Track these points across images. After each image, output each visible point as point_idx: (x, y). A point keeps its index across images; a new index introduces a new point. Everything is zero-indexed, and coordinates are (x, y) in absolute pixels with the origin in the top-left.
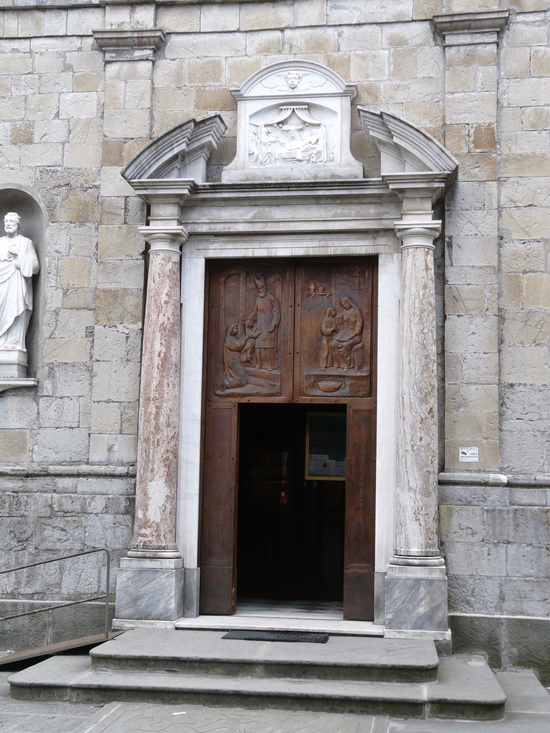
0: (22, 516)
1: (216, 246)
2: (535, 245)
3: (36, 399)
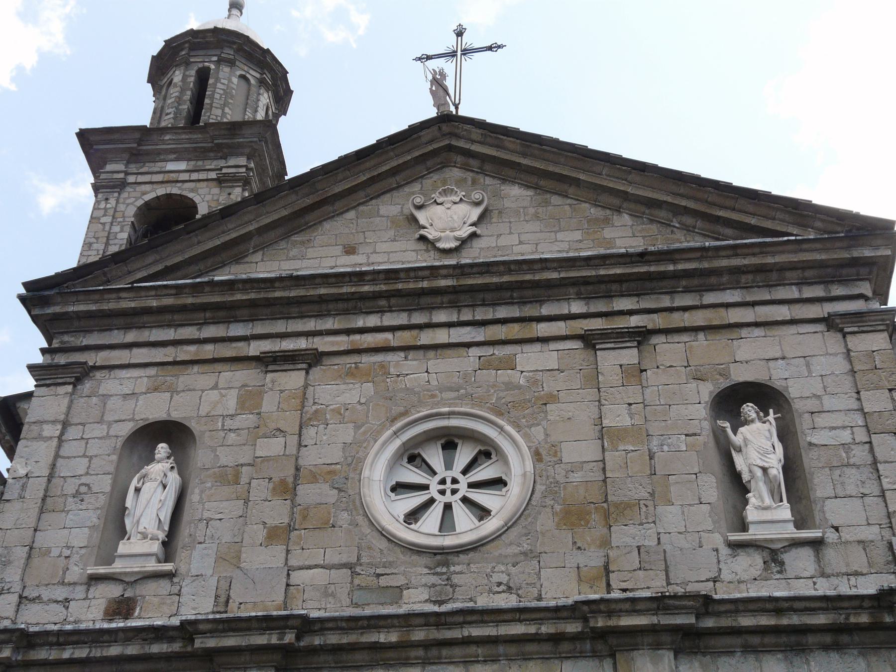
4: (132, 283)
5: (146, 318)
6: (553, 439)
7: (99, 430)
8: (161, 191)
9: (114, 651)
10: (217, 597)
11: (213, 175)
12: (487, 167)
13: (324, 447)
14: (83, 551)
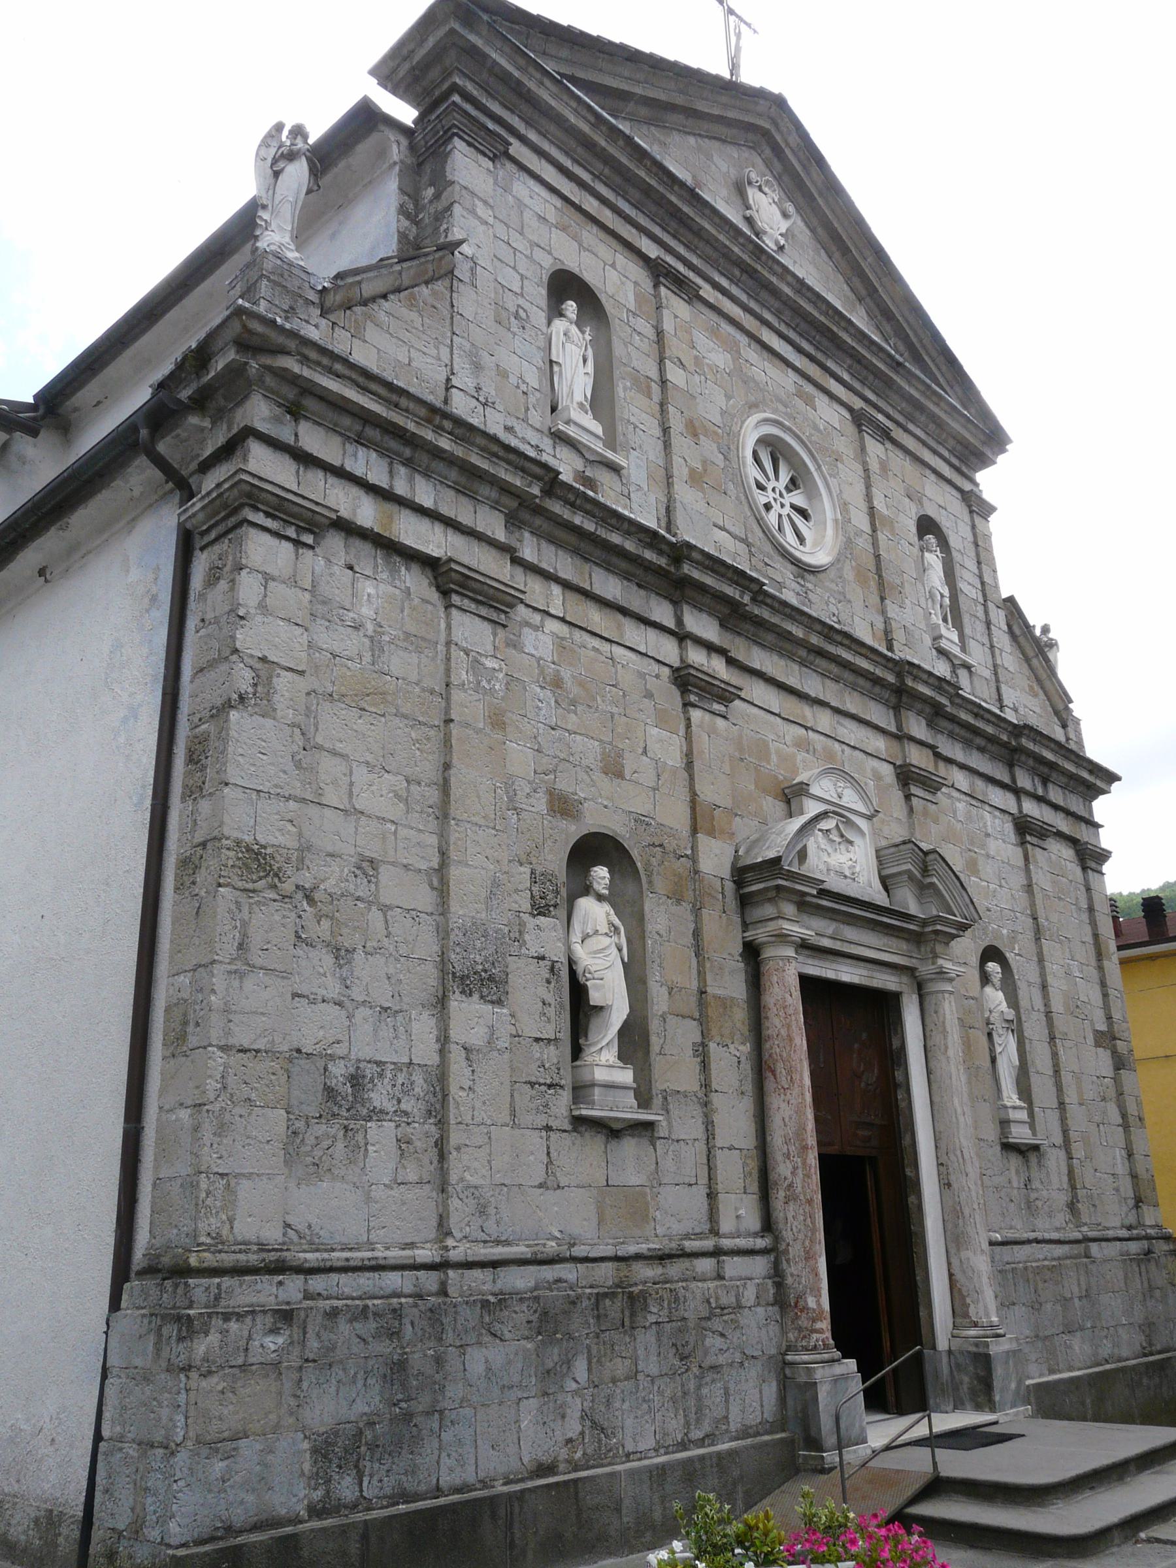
0: (684, 1319)
4: (562, 75)
5: (552, 128)
9: (615, 538)
10: (658, 519)
12: (786, 178)
14: (538, 394)
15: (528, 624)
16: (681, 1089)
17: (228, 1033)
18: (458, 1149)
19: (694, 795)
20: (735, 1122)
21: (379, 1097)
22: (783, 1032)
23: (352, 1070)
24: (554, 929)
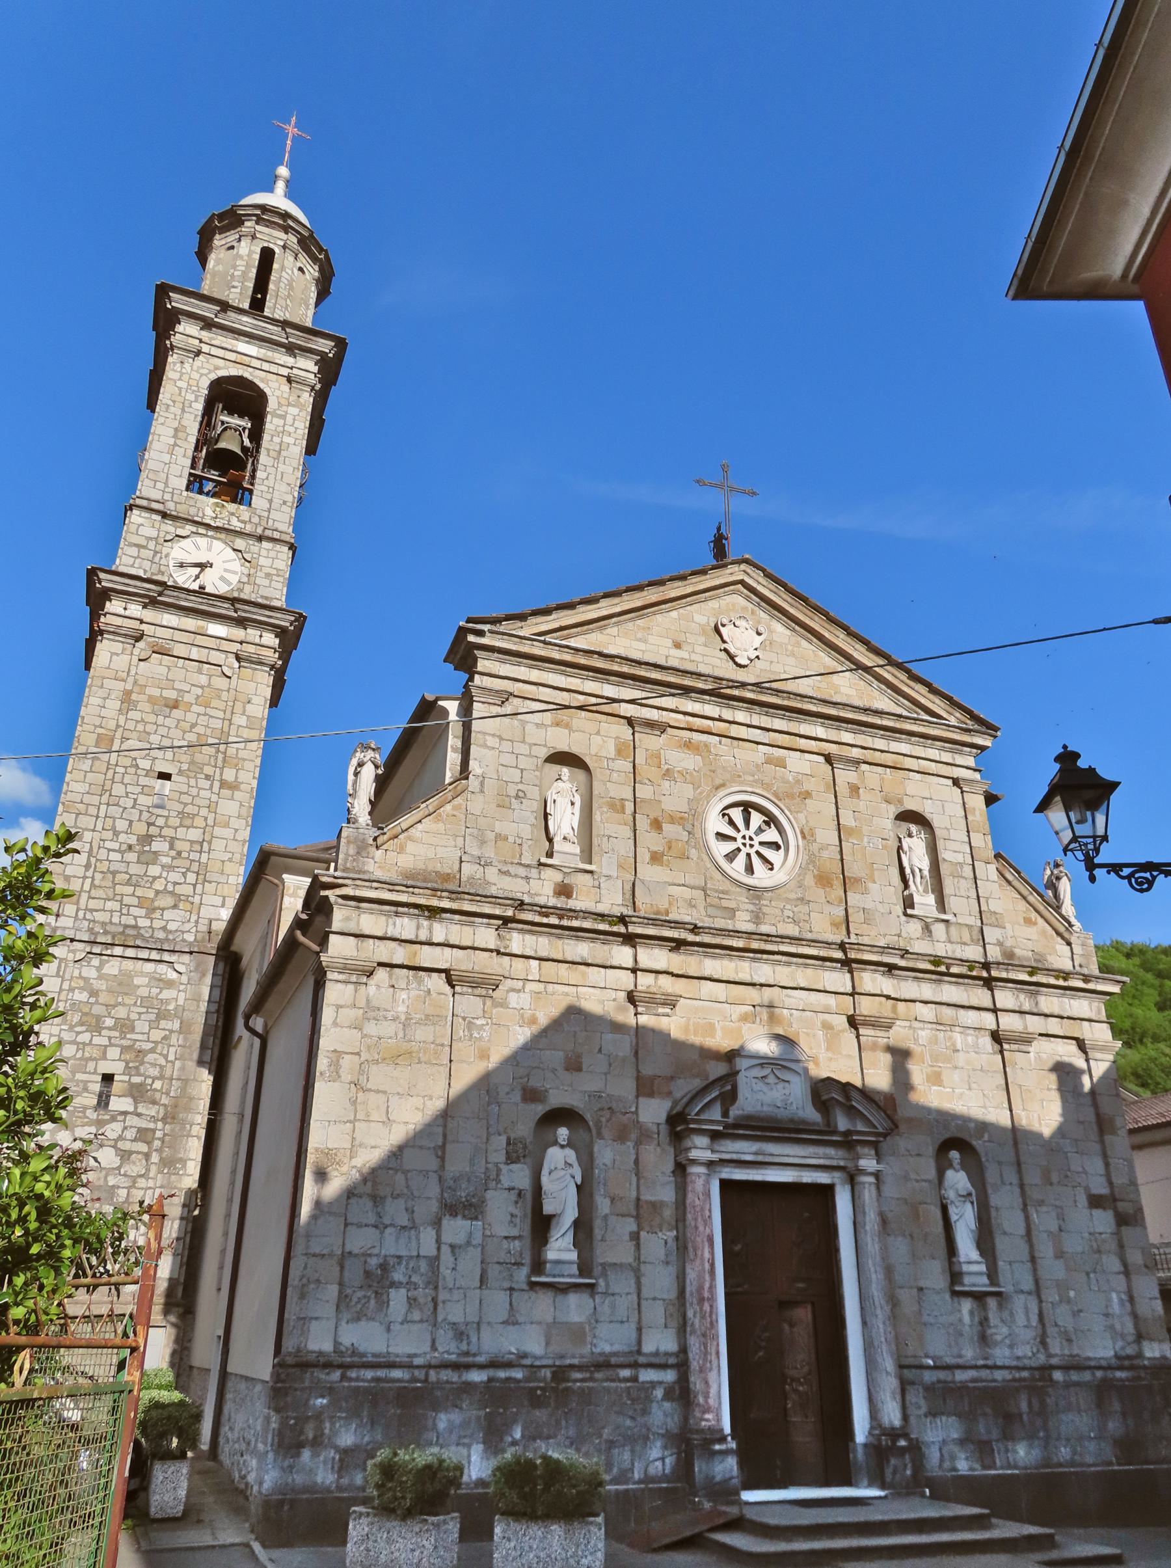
1: (727, 1170)
2: (924, 1184)
3: (592, 1296)
6: (811, 824)
7: (523, 749)
8: (234, 371)
10: (623, 894)
11: (285, 372)
13: (675, 797)
14: (530, 842)
15: (513, 990)
16: (618, 1262)
17: (307, 1247)
18: (444, 1302)
19: (638, 1071)
20: (659, 1281)
21: (398, 1276)
22: (693, 1224)
23: (381, 1261)
24: (522, 1170)
